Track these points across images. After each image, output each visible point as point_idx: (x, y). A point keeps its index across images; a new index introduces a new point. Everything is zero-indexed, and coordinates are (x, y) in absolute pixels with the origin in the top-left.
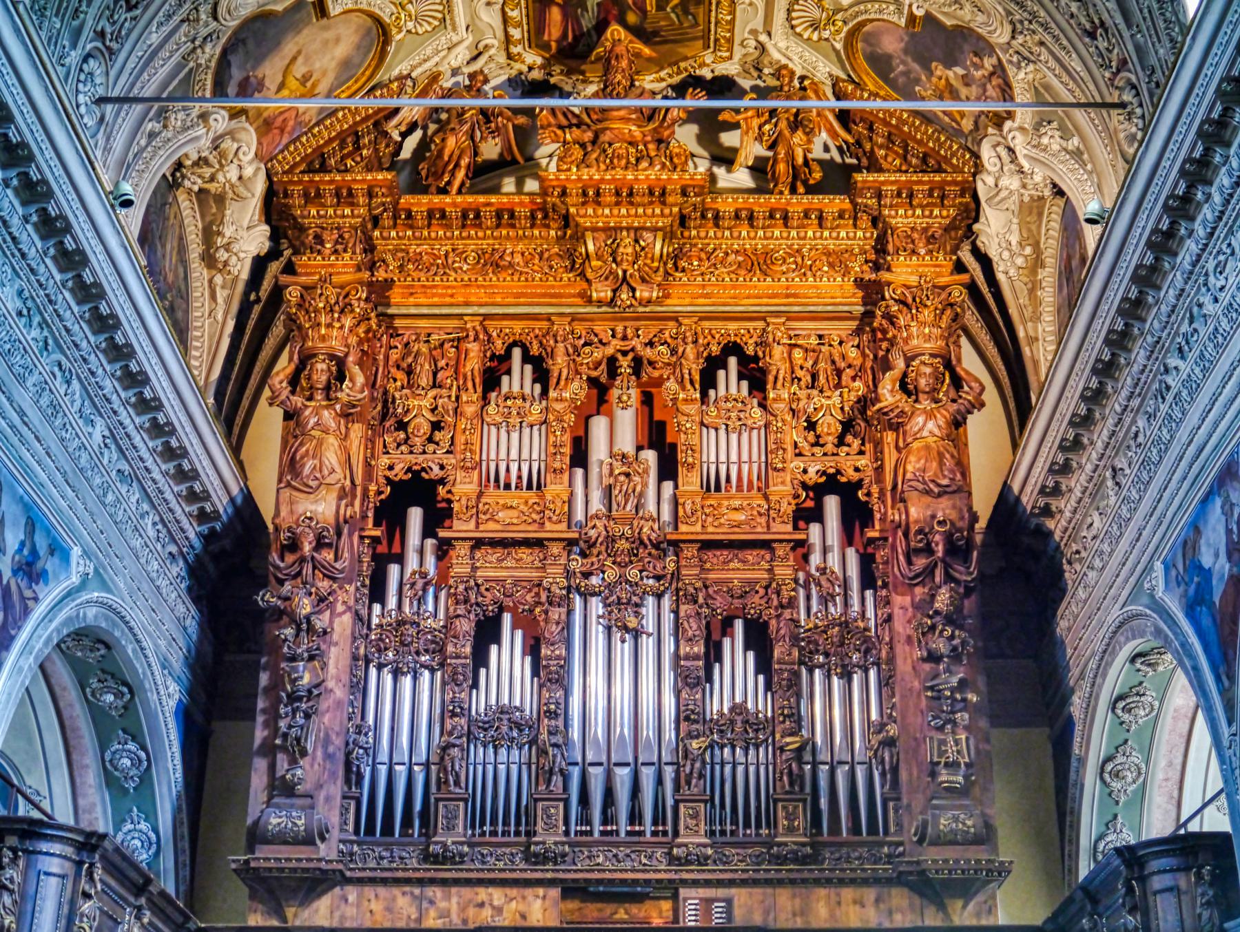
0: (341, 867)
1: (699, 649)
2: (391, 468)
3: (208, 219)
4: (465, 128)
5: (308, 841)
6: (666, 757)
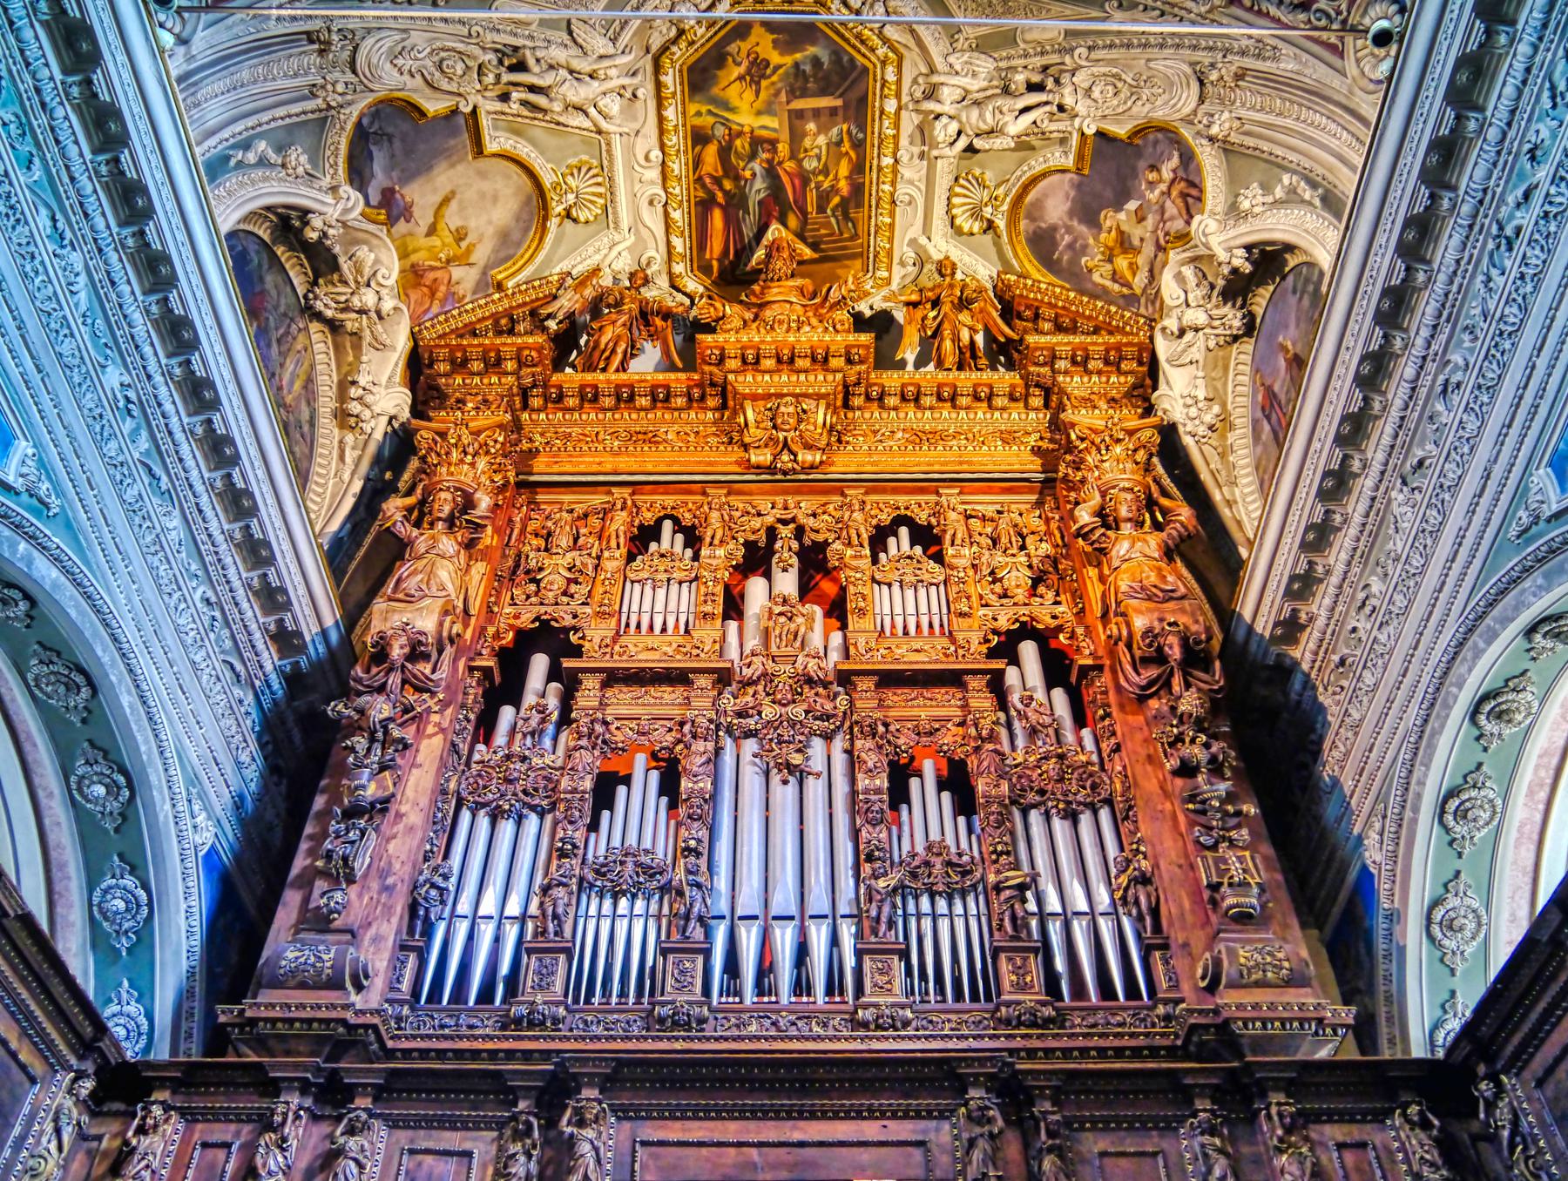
0: (376, 1020)
1: (882, 782)
2: (517, 617)
3: (345, 369)
4: (624, 318)
5: (335, 984)
6: (844, 908)
